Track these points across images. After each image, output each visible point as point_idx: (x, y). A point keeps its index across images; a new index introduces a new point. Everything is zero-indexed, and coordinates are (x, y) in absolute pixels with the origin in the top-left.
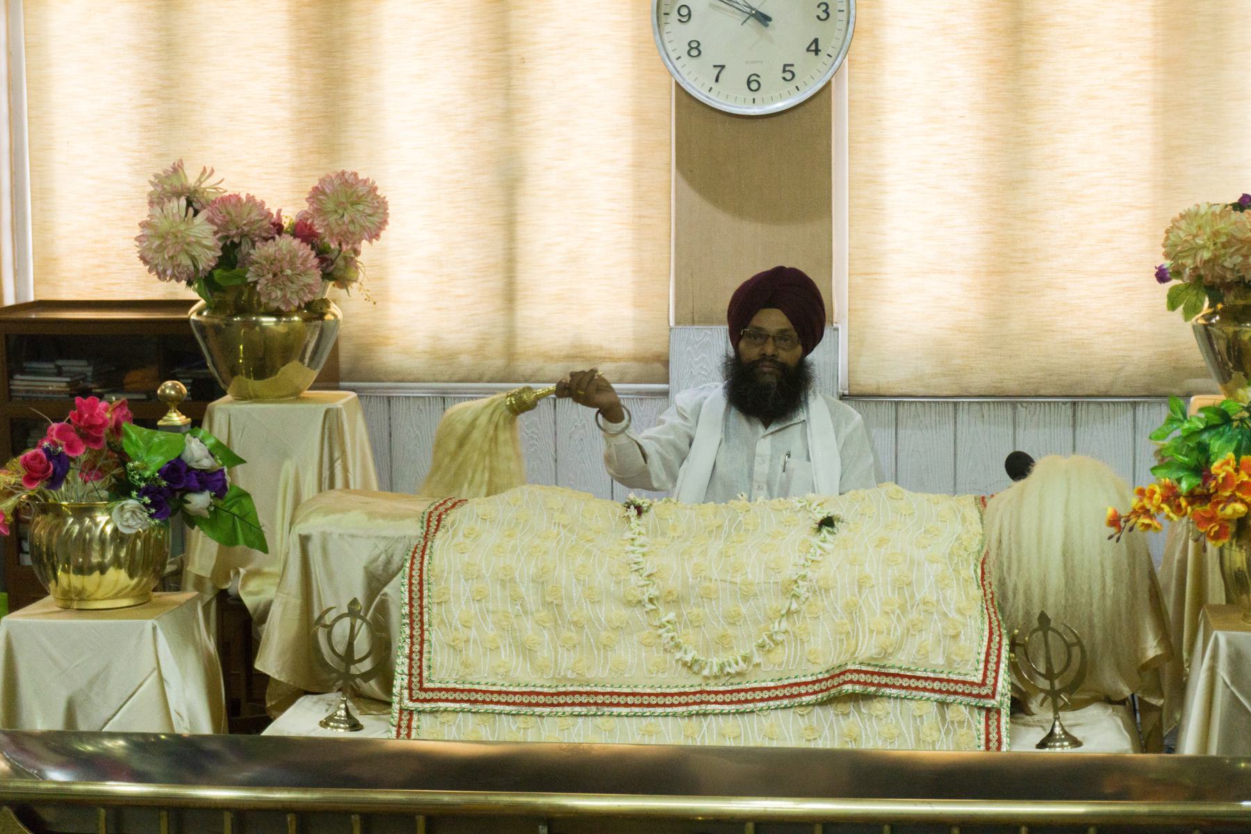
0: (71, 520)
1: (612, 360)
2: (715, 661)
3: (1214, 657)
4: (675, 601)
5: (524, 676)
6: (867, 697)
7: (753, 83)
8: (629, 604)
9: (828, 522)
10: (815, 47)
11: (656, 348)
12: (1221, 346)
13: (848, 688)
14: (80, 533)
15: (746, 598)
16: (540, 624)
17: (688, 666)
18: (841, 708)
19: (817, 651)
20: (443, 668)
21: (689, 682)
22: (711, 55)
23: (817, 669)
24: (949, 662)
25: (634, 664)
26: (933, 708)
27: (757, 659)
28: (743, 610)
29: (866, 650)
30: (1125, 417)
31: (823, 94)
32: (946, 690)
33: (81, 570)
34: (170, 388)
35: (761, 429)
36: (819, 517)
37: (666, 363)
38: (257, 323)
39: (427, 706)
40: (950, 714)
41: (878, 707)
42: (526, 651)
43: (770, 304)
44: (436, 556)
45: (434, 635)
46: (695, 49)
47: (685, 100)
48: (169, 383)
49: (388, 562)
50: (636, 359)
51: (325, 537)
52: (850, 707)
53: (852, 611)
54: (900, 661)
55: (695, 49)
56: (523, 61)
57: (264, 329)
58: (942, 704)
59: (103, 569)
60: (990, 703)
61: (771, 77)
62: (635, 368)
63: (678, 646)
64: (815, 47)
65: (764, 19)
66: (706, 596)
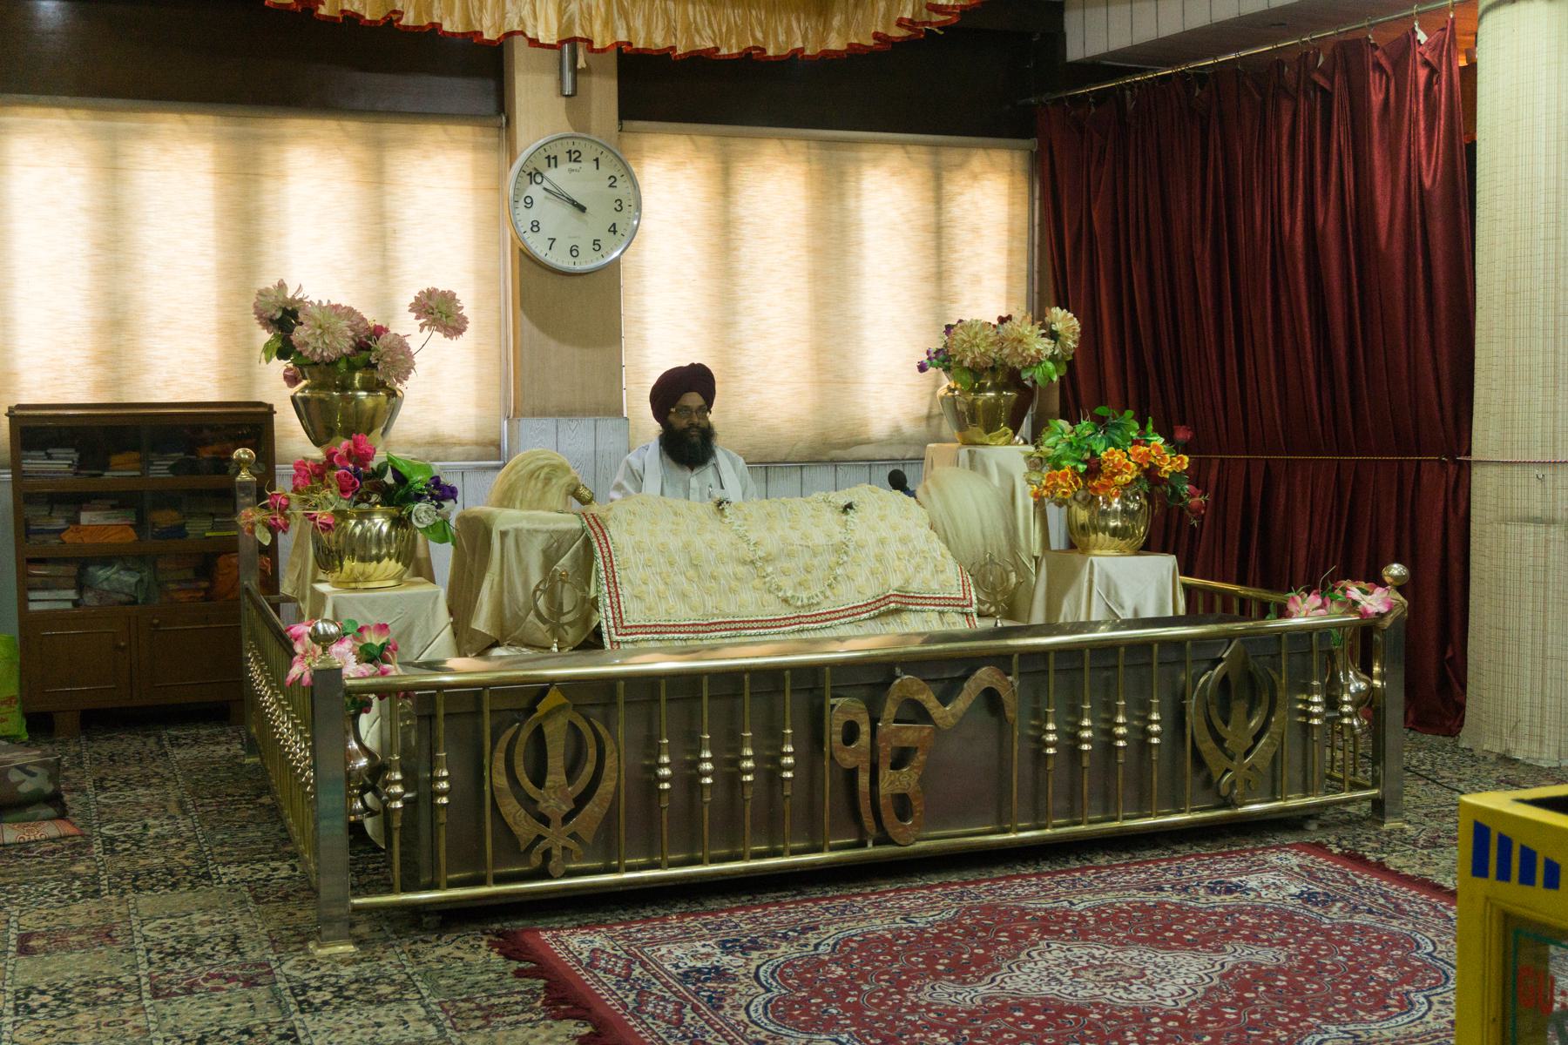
0: (353, 522)
1: (461, 444)
2: (804, 595)
3: (1091, 573)
4: (767, 560)
5: (682, 614)
6: (897, 611)
7: (574, 251)
8: (744, 563)
9: (849, 507)
10: (613, 229)
11: (494, 436)
12: (962, 407)
13: (892, 606)
14: (362, 533)
15: (815, 555)
16: (690, 580)
17: (785, 601)
18: (884, 620)
19: (860, 587)
20: (635, 613)
21: (785, 612)
22: (548, 229)
23: (869, 594)
24: (943, 586)
25: (749, 602)
26: (936, 615)
27: (828, 593)
28: (816, 562)
29: (895, 582)
30: (796, 476)
31: (617, 261)
32: (943, 604)
33: (363, 559)
34: (241, 453)
35: (688, 473)
36: (843, 503)
37: (499, 447)
38: (355, 398)
39: (629, 638)
40: (947, 618)
41: (905, 616)
42: (684, 596)
43: (690, 390)
44: (616, 539)
45: (625, 591)
46: (535, 226)
47: (527, 259)
48: (241, 450)
49: (559, 547)
50: (477, 444)
51: (518, 531)
52: (890, 619)
53: (880, 559)
54: (914, 587)
55: (535, 226)
56: (395, 231)
57: (358, 402)
58: (941, 613)
59: (379, 559)
60: (968, 610)
61: (585, 246)
62: (475, 450)
63: (779, 589)
64: (613, 229)
65: (582, 209)
66: (790, 555)
